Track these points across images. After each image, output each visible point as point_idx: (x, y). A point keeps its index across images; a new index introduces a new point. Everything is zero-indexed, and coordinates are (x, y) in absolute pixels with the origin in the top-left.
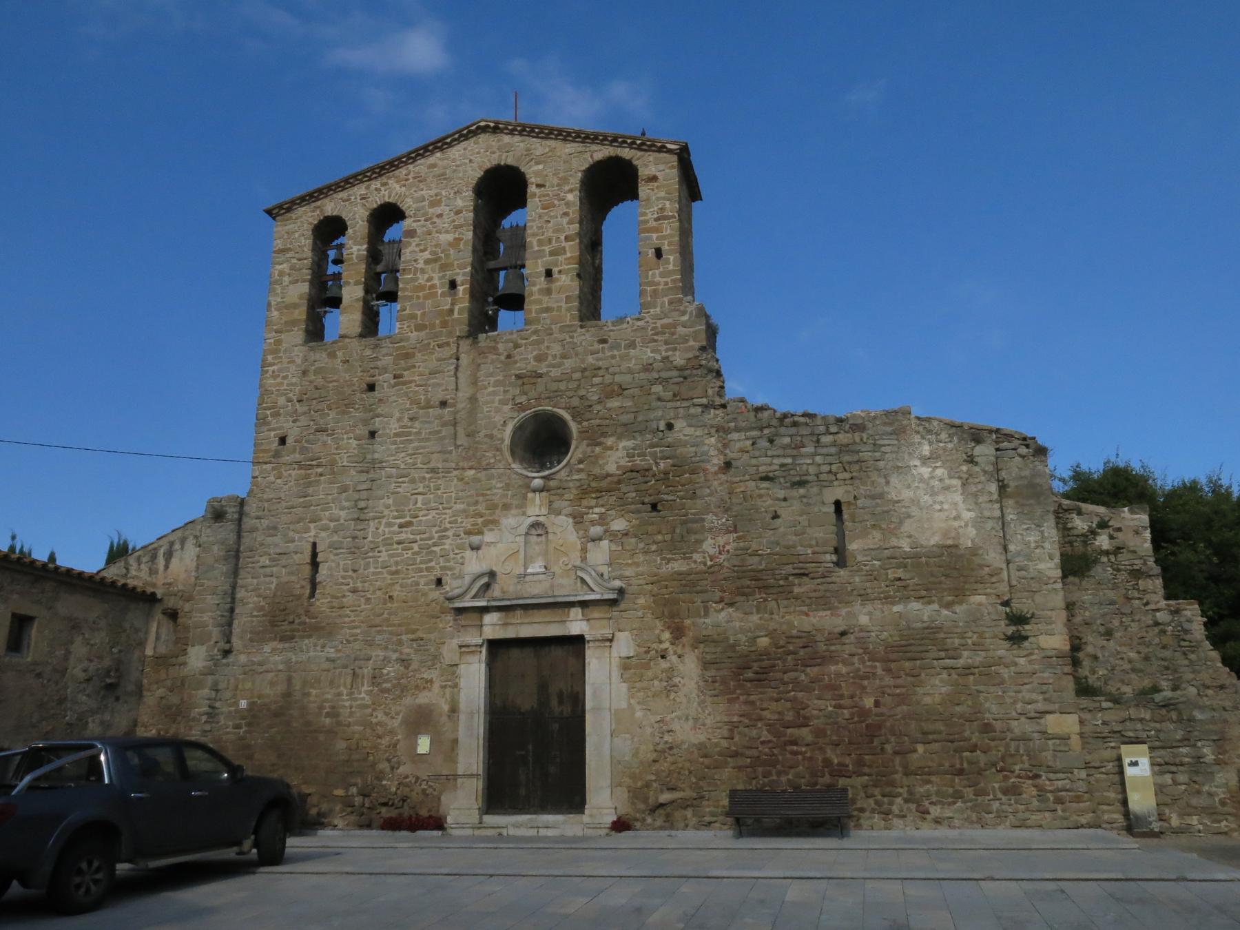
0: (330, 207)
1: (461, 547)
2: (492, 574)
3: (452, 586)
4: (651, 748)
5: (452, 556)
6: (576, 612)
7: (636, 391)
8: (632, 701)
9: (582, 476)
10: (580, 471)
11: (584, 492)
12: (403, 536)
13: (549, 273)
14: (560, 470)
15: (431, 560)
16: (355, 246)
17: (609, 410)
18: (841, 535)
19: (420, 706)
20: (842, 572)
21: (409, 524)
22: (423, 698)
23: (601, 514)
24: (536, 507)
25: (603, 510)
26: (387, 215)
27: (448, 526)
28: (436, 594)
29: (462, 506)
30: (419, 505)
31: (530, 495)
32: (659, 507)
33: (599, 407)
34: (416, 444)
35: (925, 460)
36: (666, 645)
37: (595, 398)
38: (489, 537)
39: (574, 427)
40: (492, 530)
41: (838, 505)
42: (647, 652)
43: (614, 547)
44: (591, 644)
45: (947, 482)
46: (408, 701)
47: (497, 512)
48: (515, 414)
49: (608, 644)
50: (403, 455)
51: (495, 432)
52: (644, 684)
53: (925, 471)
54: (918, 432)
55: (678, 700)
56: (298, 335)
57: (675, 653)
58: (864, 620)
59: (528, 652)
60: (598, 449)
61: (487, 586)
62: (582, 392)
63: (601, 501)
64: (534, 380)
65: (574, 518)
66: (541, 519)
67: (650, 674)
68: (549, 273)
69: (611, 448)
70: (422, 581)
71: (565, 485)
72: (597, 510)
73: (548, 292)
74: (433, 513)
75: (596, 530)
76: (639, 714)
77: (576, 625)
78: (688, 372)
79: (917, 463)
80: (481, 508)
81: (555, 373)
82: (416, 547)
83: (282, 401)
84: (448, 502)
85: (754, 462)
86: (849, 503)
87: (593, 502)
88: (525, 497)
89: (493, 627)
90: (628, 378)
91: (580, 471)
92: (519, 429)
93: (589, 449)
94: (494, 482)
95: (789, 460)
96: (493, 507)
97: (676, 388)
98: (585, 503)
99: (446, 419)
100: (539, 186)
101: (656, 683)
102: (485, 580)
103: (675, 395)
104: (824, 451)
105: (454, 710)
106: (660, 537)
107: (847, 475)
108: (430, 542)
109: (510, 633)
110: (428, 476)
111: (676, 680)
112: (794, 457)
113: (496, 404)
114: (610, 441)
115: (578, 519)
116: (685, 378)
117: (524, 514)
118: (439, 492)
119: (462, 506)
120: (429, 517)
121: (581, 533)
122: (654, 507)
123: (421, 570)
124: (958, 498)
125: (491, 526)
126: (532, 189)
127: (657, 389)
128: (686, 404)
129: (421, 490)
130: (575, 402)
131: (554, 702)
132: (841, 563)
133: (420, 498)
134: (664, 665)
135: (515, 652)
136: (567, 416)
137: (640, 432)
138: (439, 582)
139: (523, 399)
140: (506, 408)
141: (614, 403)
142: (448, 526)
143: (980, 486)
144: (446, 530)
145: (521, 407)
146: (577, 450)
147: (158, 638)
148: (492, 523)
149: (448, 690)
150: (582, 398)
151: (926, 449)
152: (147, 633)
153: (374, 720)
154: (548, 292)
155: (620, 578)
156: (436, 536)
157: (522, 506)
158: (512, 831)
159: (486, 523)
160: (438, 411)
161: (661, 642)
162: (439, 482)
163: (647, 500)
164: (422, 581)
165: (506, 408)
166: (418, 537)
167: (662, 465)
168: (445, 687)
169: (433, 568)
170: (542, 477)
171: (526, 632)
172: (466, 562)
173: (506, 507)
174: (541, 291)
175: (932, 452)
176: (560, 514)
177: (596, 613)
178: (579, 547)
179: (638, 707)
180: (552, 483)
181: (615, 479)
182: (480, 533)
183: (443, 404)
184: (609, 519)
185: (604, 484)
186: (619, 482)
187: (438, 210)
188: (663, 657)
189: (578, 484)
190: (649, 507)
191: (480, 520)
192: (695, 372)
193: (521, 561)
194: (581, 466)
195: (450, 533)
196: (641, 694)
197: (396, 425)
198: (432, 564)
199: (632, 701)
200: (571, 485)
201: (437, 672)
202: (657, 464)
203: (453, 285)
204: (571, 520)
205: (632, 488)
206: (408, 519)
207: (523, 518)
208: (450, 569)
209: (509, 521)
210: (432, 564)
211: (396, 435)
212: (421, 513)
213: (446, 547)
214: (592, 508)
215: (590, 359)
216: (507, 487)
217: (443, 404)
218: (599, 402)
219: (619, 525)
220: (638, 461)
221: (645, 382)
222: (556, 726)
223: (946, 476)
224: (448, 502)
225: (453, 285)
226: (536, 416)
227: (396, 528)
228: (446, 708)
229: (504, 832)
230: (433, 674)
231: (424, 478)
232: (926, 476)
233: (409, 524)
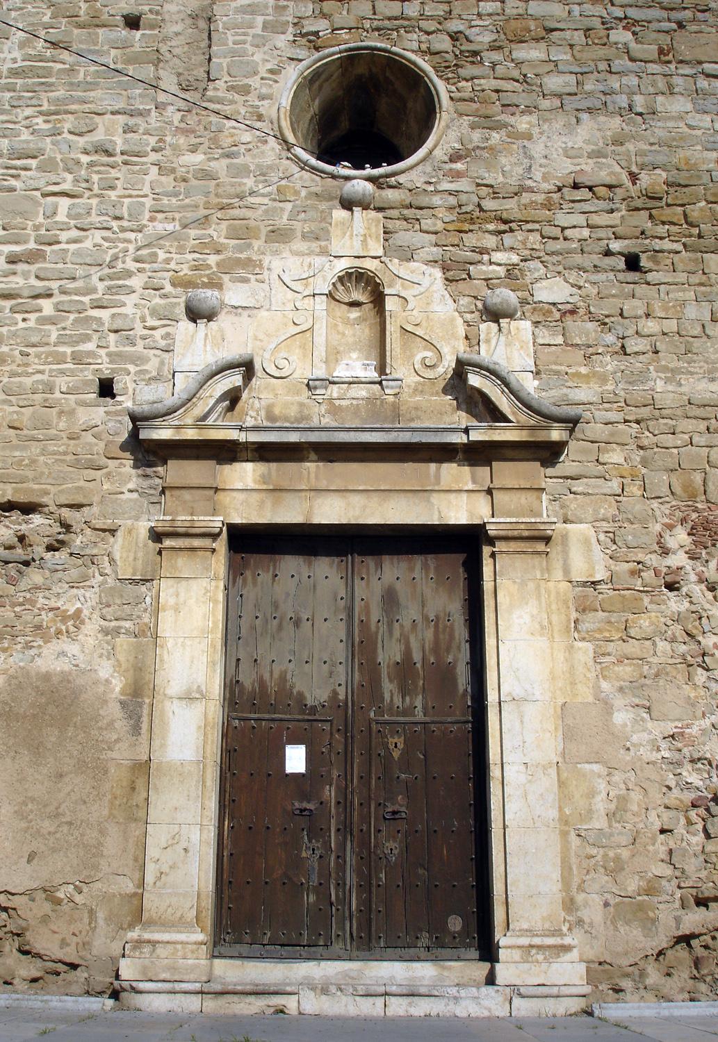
1: (168, 318)
2: (247, 368)
3: (136, 394)
5: (139, 331)
6: (452, 473)
7: (578, 37)
8: (605, 685)
9: (463, 185)
10: (458, 175)
11: (468, 218)
12: (17, 282)
14: (413, 171)
15: (87, 338)
17: (519, 64)
19: (47, 677)
21: (32, 257)
22: (52, 658)
24: (355, 239)
25: (515, 259)
27: (132, 266)
28: (97, 412)
29: (170, 227)
30: (61, 217)
31: (340, 214)
32: (644, 262)
33: (496, 56)
34: (61, 93)
36: (679, 559)
37: (487, 38)
38: (234, 294)
40: (246, 281)
42: (635, 573)
43: (545, 336)
44: (500, 546)
47: (256, 244)
48: (301, 53)
49: (541, 547)
50: (29, 112)
51: (254, 82)
52: (632, 648)
59: (326, 572)
60: (496, 137)
61: (233, 398)
62: (454, 25)
63: (508, 239)
65: (445, 269)
67: (644, 624)
69: (529, 137)
70: (62, 383)
71: (424, 200)
72: (498, 257)
74: (98, 236)
76: (621, 717)
77: (455, 500)
78: (688, 14)
80: (218, 232)
82: (47, 306)
84: (133, 216)
87: (490, 241)
88: (325, 218)
89: (246, 494)
91: (458, 175)
92: (312, 81)
93: (476, 136)
94: (249, 182)
96: (243, 233)
97: (665, 40)
98: (470, 240)
99: (137, 48)
101: (662, 646)
102: (236, 379)
103: (661, 52)
106: (651, 326)
108: (86, 299)
109: (289, 513)
110: (85, 159)
113: (259, 31)
114: (523, 123)
115: (455, 273)
116: (681, 25)
117: (324, 252)
118: (113, 195)
119: (170, 227)
120: (88, 244)
121: (464, 301)
122: (633, 263)
123: (60, 359)
125: (242, 273)
127: (621, 36)
128: (687, 70)
129: (66, 187)
130: (442, 43)
131: (389, 688)
133: (64, 202)
134: (675, 604)
135: (291, 565)
136: (424, 64)
137: (589, 110)
138: (106, 389)
139: (322, 26)
140: (282, 41)
142: (132, 266)
144: (128, 274)
145: (314, 41)
146: (447, 133)
148: (242, 268)
149: (122, 641)
150: (454, 37)
156: (101, 286)
157: (318, 236)
158: (311, 1004)
159: (228, 267)
160: (125, 33)
161: (665, 552)
162: (114, 173)
163: (615, 246)
164: (62, 383)
165: (282, 41)
166: (54, 285)
167: (645, 179)
168: (117, 631)
169: (90, 354)
170: (370, 179)
171: (331, 511)
172: (178, 348)
173: (279, 235)
176: (411, 259)
177: (507, 472)
178: (461, 330)
179: (619, 701)
180: (391, 195)
181: (540, 198)
182: (216, 285)
183: (133, 22)
184: (528, 280)
185: (511, 207)
186: (548, 205)
188: (671, 587)
189: (452, 201)
190: (621, 264)
191: (213, 259)
192: (699, 14)
193: (320, 351)
194: (459, 166)
195: (136, 282)
196: (626, 670)
197: (17, 54)
198: (90, 346)
199: (605, 685)
200: (436, 200)
201: (92, 596)
202: (634, 177)
204: (438, 273)
205: (581, 220)
206: (32, 245)
207: (319, 261)
208: (137, 360)
209: (287, 263)
210: (90, 346)
211: (14, 73)
212: (64, 236)
213: (128, 310)
216: (281, 196)
217: (133, 22)
218: (494, 47)
219: (553, 290)
220: (587, 165)
221: (596, 23)
222: (396, 744)
224: (133, 216)
226: (351, 59)
229: (291, 1004)
230: (83, 600)
231: (78, 162)
233: (32, 257)
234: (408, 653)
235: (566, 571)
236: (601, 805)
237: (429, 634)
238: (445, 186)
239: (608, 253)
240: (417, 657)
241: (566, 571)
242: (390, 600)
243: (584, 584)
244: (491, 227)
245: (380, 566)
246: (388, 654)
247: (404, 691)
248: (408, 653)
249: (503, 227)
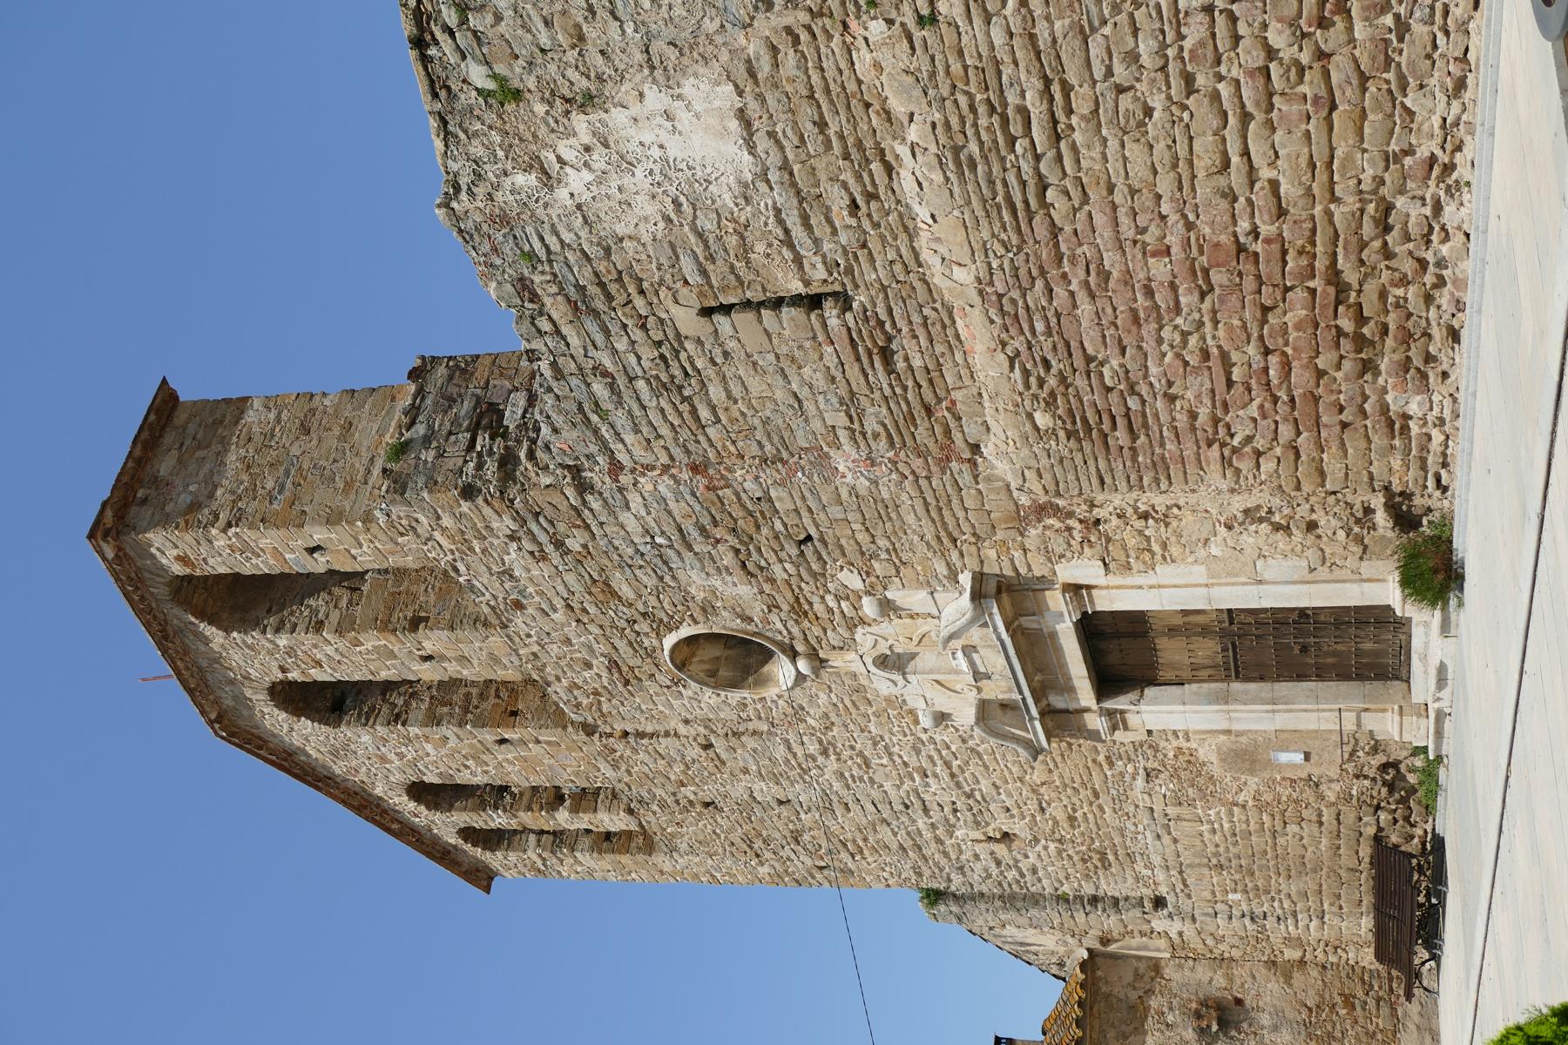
4: (1280, 535)
9: (773, 617)
13: (429, 658)
16: (498, 820)
18: (777, 303)
20: (860, 299)
23: (838, 598)
35: (548, 180)
39: (686, 631)
41: (707, 312)
45: (586, 138)
46: (1216, 770)
53: (577, 181)
54: (490, 197)
56: (660, 859)
58: (964, 276)
64: (625, 669)
66: (869, 661)
68: (429, 658)
75: (869, 607)
79: (562, 194)
81: (602, 648)
85: (664, 431)
86: (701, 294)
90: (571, 578)
95: (640, 384)
100: (283, 670)
104: (599, 338)
105: (1228, 732)
107: (639, 302)
112: (631, 380)
124: (618, 117)
126: (295, 675)
136: (670, 641)
141: (626, 591)
143: (570, 73)
147: (1146, 948)
151: (526, 180)
152: (1139, 958)
153: (1251, 803)
154: (463, 659)
155: (953, 576)
175: (528, 169)
187: (392, 756)
203: (503, 741)
214: (830, 611)
215: (559, 616)
219: (854, 581)
223: (572, 141)
225: (503, 741)
227: (931, 780)
228: (1223, 738)
232: (587, 176)
238: (779, 625)
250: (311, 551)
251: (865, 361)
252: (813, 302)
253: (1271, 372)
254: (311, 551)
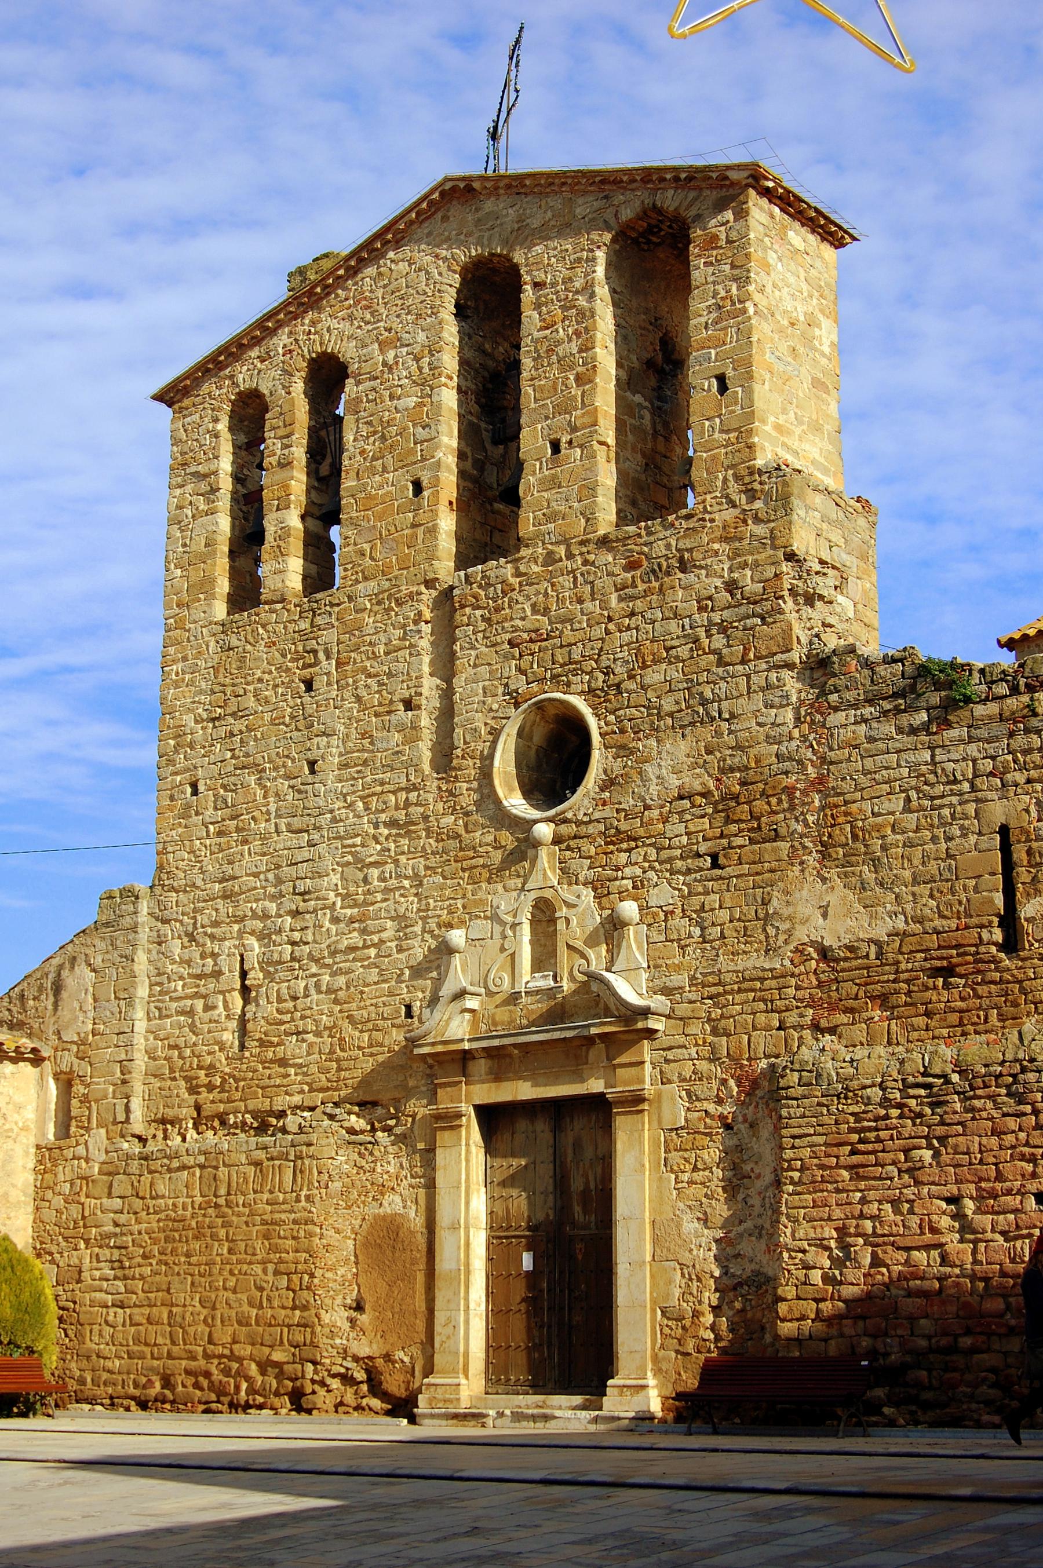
0: (244, 375)
19: (384, 1218)
26: (327, 376)
32: (722, 861)
39: (592, 722)
41: (1004, 831)
55: (750, 1202)
57: (745, 1120)
73: (554, 483)
83: (189, 720)
111: (747, 1167)
131: (577, 1209)
132: (1011, 944)
141: (654, 676)
163: (703, 848)
174: (542, 482)
234: (587, 1183)
235: (660, 1122)
236: (677, 1292)
237: (599, 1170)
239: (698, 855)
240: (592, 1186)
241: (660, 1122)
242: (577, 1145)
243: (671, 1130)
244: (624, 846)
245: (572, 1121)
246: (577, 1185)
247: (585, 1212)
248: (587, 1183)
249: (633, 844)
250: (721, 379)
251: (944, 953)
252: (1009, 920)
253: (918, 1282)
254: (721, 379)
